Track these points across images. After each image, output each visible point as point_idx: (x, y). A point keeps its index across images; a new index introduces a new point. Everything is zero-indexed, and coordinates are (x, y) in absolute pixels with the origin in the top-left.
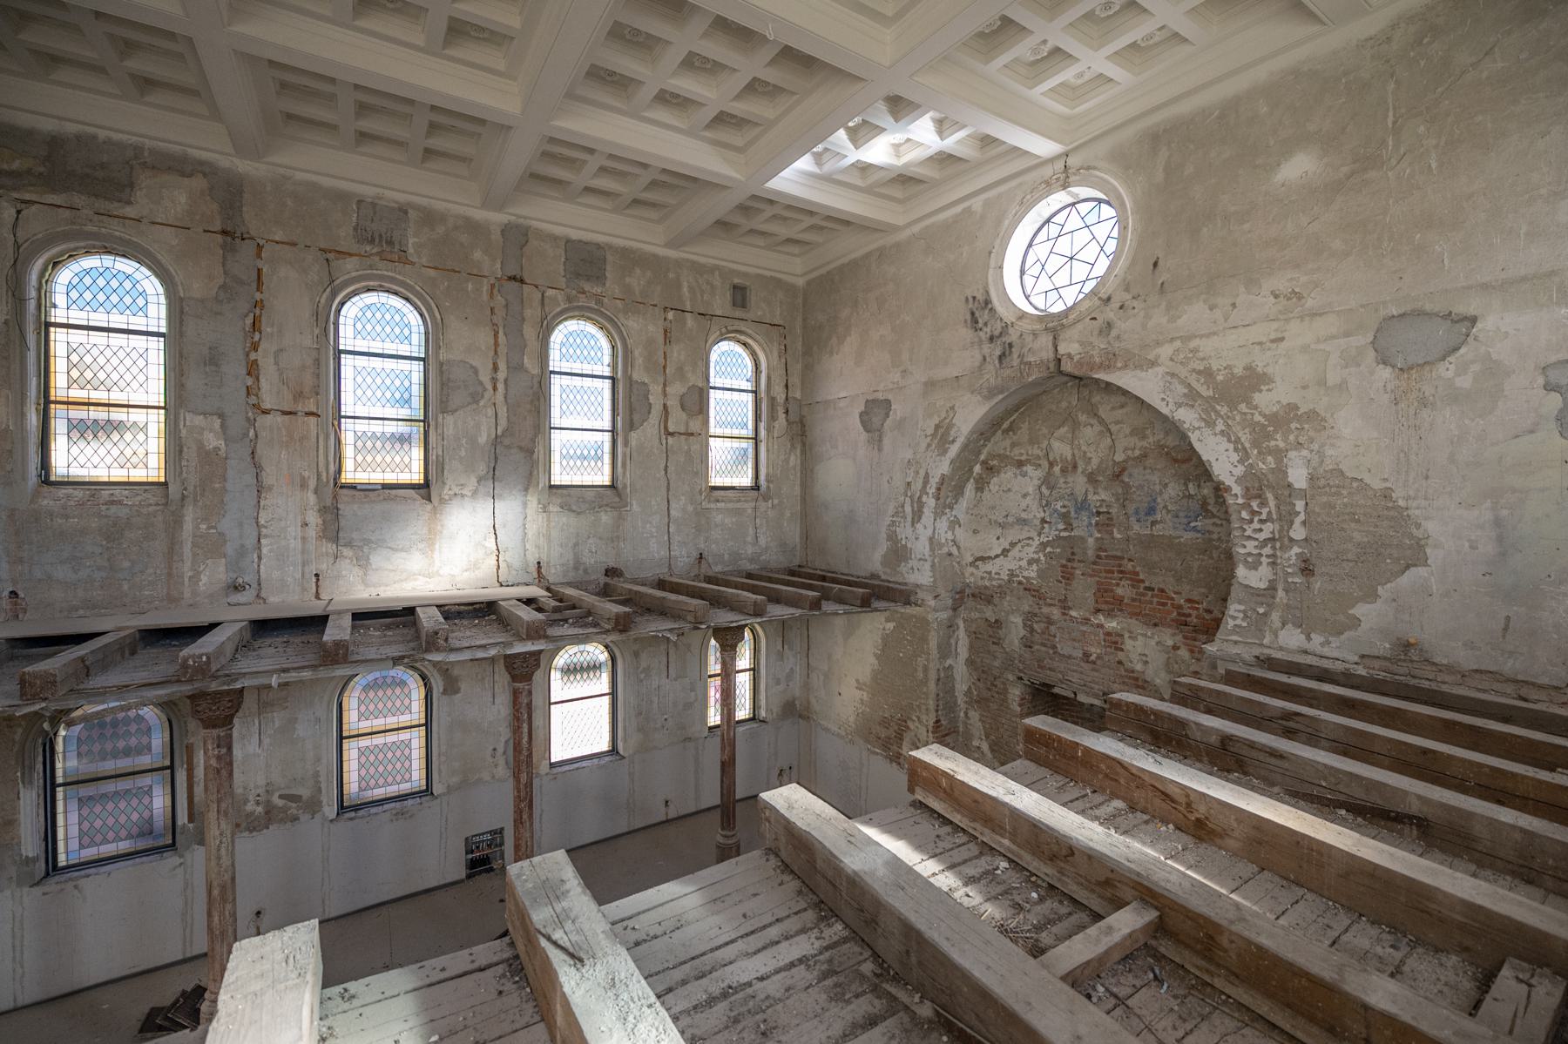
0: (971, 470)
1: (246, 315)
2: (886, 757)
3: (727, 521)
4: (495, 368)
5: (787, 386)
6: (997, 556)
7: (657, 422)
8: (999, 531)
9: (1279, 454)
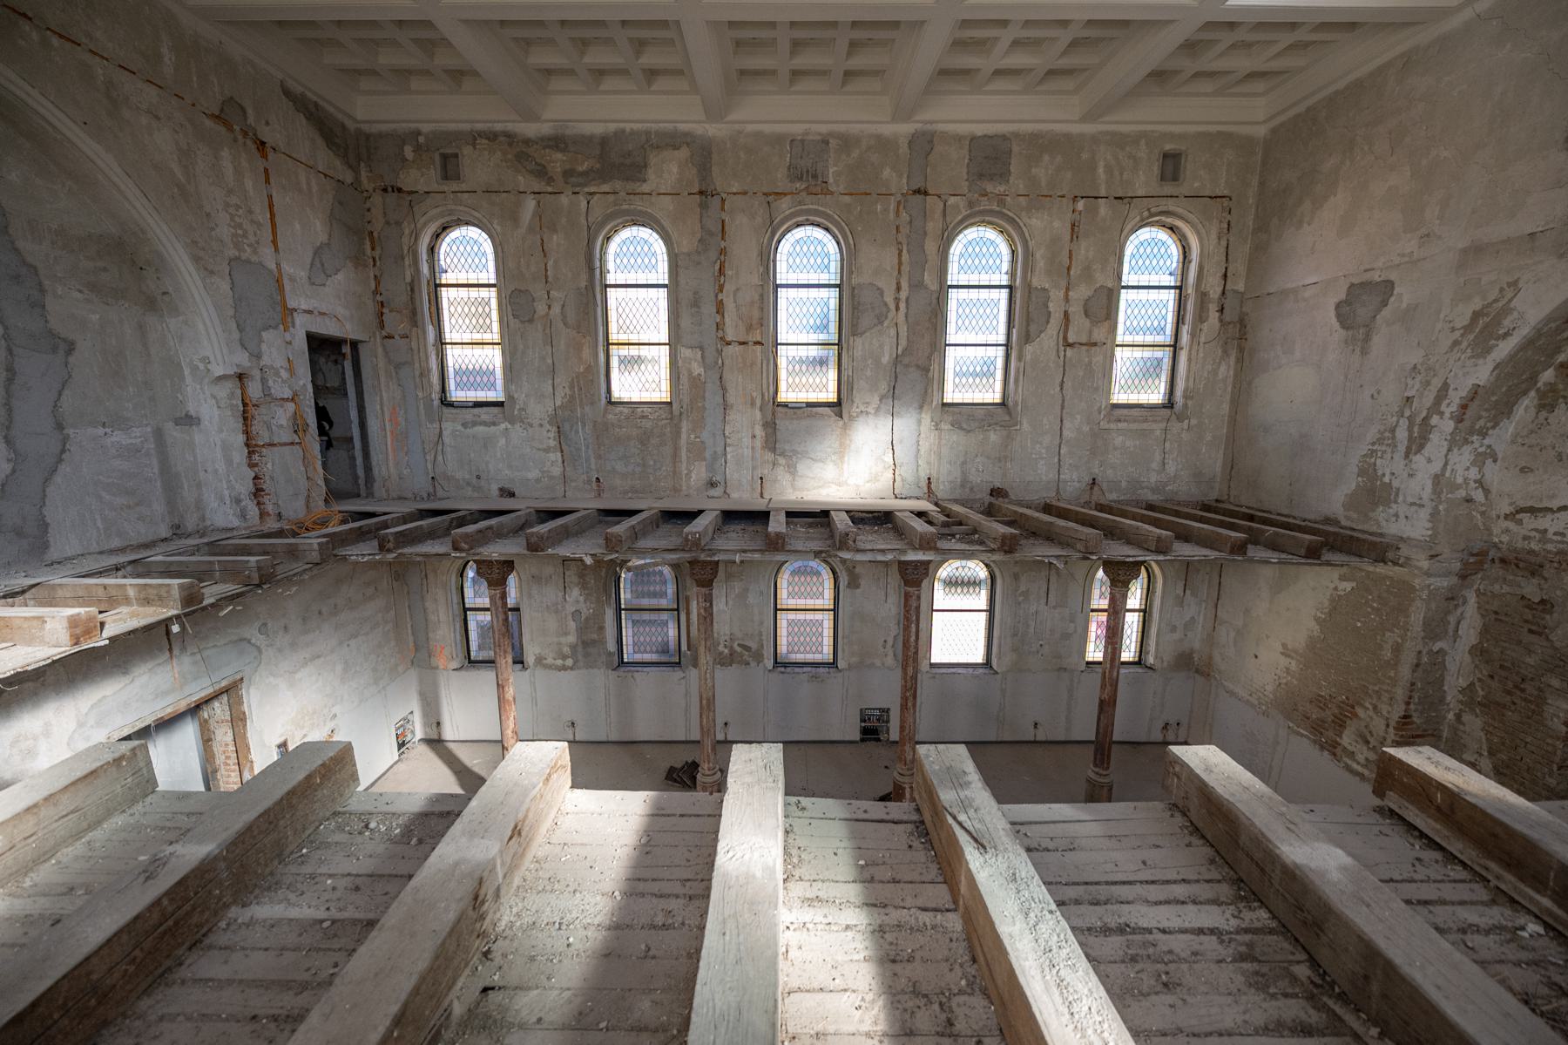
0: (1533, 379)
1: (715, 262)
2: (1315, 742)
3: (1128, 443)
4: (899, 289)
5: (1225, 276)
7: (1055, 333)
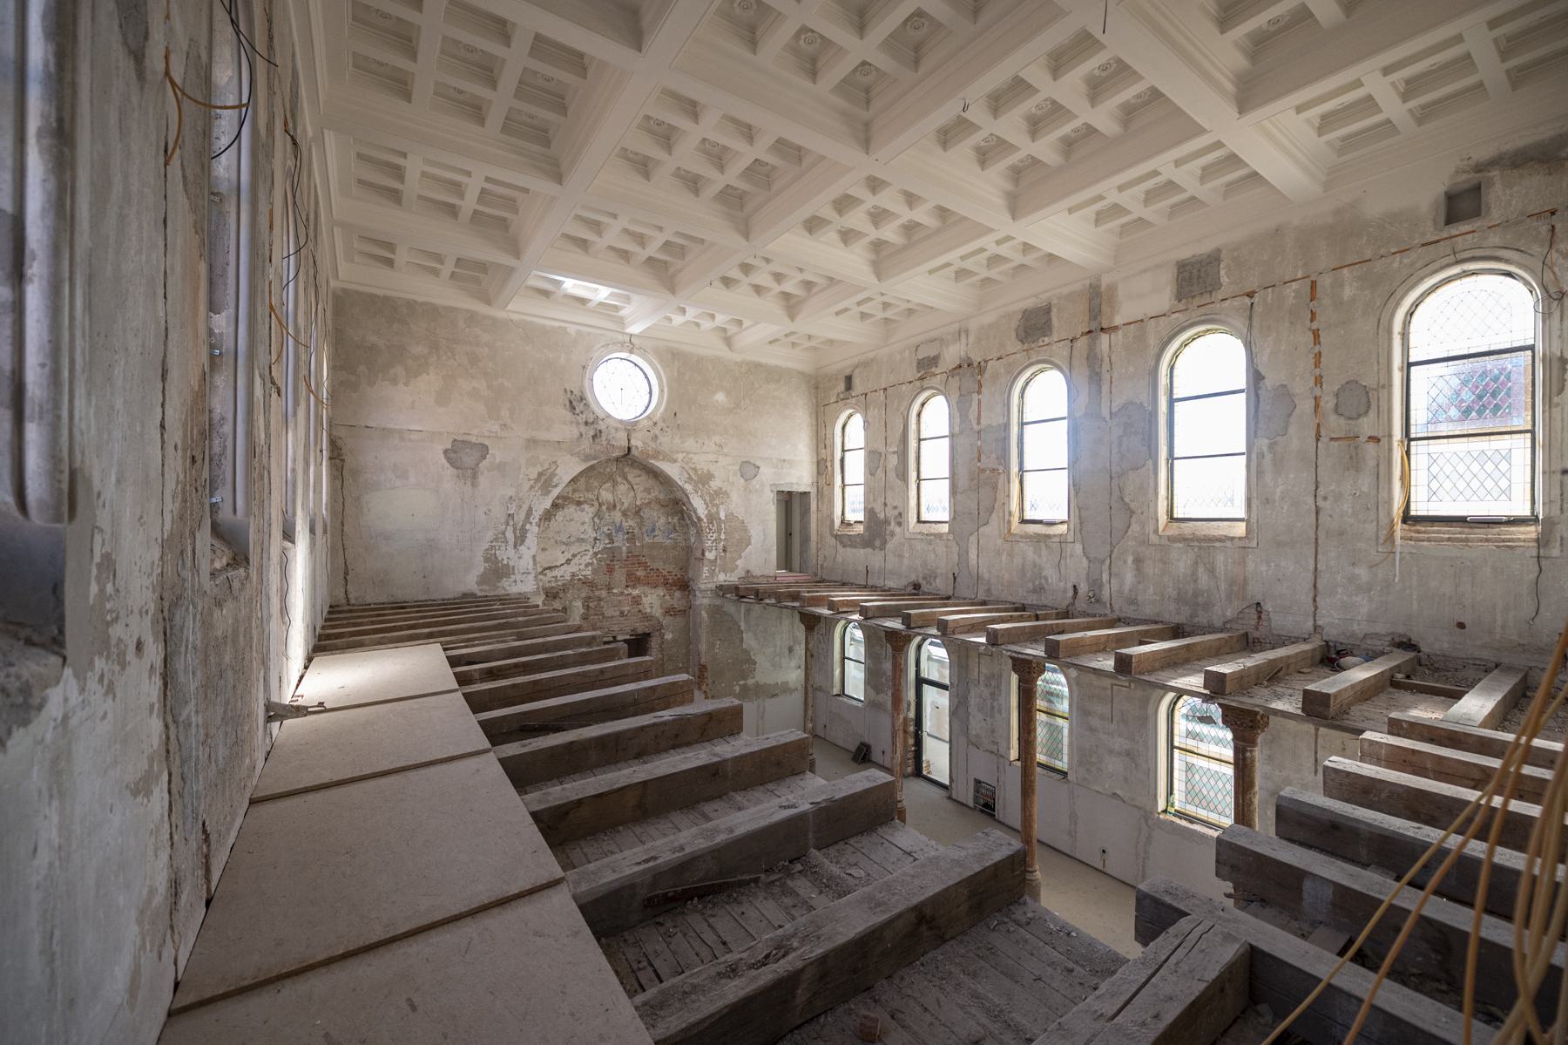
6: (562, 565)
8: (564, 548)
9: (717, 506)
